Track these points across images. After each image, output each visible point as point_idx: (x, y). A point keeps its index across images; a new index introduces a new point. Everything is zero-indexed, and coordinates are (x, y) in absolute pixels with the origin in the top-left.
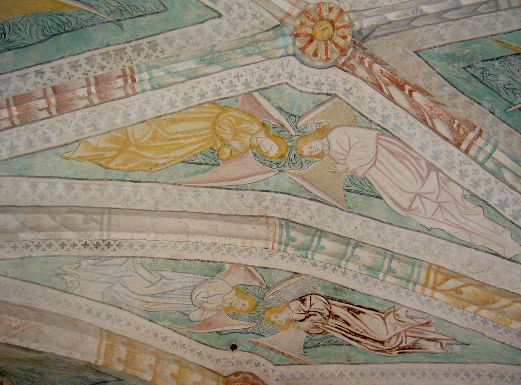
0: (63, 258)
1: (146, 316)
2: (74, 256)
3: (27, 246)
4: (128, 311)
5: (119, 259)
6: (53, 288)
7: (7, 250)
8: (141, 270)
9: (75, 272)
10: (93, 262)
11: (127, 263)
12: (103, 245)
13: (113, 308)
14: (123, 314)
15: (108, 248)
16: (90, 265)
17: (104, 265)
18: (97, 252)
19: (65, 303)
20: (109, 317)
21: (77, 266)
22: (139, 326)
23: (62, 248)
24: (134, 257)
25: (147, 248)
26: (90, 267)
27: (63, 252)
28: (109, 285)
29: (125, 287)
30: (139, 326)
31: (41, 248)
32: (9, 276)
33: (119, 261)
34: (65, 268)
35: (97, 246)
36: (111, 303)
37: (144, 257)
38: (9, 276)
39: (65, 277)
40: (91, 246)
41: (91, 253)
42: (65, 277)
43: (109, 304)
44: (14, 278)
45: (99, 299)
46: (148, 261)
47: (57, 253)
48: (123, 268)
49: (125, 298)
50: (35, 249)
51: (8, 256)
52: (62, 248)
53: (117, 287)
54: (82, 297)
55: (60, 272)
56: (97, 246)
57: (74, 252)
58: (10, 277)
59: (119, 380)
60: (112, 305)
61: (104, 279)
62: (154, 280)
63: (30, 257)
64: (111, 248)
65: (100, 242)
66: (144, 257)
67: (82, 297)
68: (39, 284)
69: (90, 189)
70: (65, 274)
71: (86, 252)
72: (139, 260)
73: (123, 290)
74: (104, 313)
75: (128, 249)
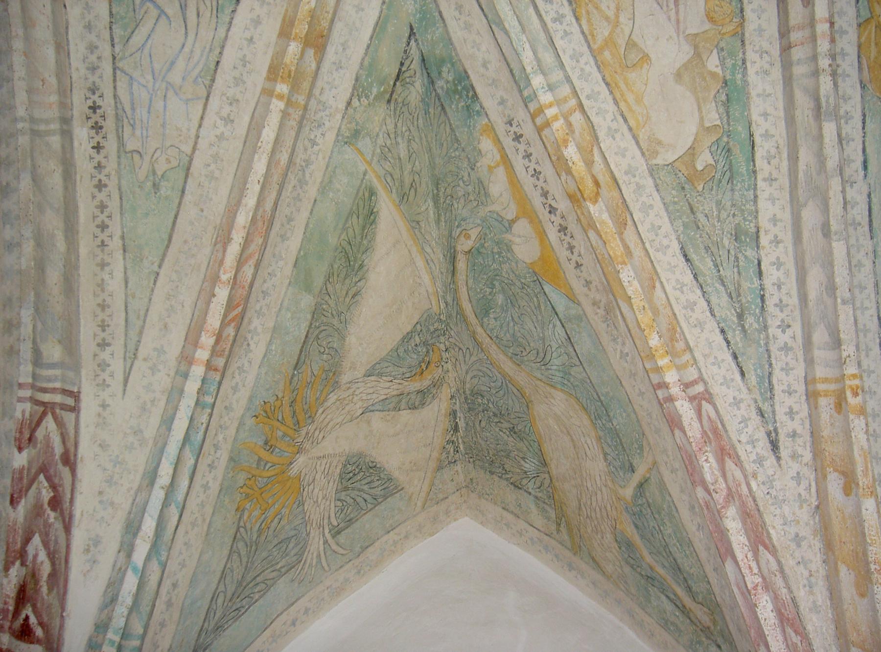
0: (123, 182)
1: (228, 11)
2: (119, 164)
3: (103, 244)
4: (223, 47)
5: (119, 84)
6: (183, 192)
7: (107, 277)
8: (137, 39)
9: (147, 158)
10: (127, 130)
11: (126, 68)
12: (95, 118)
13: (218, 77)
14: (230, 56)
15: (100, 107)
16: (133, 134)
17: (133, 109)
18: (109, 125)
19: (213, 167)
20: (239, 81)
21: (136, 157)
22: (252, 20)
23: (106, 186)
24: (114, 58)
25: (95, 39)
26: (138, 132)
27: (112, 184)
28: (170, 94)
29: (173, 63)
30: (252, 20)
31: (107, 220)
32: (156, 269)
33: (122, 85)
34: (142, 177)
35: (97, 127)
36: (207, 83)
37: (112, 39)
38: (156, 269)
39: (160, 173)
40: (98, 138)
41: (112, 137)
42: (160, 173)
43: (211, 86)
44: (162, 260)
45: (200, 108)
46: (118, 31)
47: (116, 196)
48: (136, 74)
49: (196, 59)
50: (107, 232)
51: (119, 275)
52: (106, 186)
53: (175, 77)
54: (197, 137)
55: (149, 184)
56: (97, 127)
57: (111, 166)
58: (160, 266)
59: (412, 33)
60: (213, 80)
61: (159, 105)
62: (154, 13)
63: (123, 238)
64: (99, 102)
65: (91, 123)
66: (112, 39)
67: (197, 137)
68: (176, 217)
69: (7, 157)
70: (154, 173)
71: (111, 145)
72: (117, 48)
73: (181, 64)
74: (231, 93)
75: (98, 72)
